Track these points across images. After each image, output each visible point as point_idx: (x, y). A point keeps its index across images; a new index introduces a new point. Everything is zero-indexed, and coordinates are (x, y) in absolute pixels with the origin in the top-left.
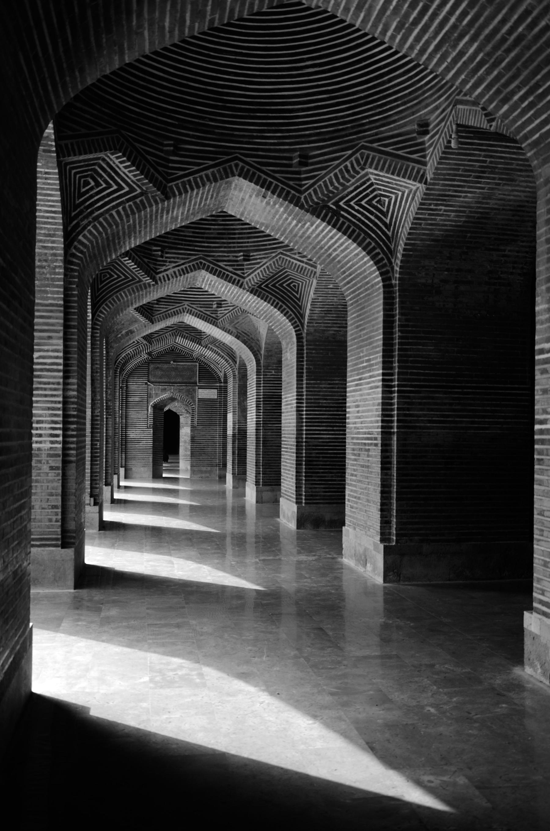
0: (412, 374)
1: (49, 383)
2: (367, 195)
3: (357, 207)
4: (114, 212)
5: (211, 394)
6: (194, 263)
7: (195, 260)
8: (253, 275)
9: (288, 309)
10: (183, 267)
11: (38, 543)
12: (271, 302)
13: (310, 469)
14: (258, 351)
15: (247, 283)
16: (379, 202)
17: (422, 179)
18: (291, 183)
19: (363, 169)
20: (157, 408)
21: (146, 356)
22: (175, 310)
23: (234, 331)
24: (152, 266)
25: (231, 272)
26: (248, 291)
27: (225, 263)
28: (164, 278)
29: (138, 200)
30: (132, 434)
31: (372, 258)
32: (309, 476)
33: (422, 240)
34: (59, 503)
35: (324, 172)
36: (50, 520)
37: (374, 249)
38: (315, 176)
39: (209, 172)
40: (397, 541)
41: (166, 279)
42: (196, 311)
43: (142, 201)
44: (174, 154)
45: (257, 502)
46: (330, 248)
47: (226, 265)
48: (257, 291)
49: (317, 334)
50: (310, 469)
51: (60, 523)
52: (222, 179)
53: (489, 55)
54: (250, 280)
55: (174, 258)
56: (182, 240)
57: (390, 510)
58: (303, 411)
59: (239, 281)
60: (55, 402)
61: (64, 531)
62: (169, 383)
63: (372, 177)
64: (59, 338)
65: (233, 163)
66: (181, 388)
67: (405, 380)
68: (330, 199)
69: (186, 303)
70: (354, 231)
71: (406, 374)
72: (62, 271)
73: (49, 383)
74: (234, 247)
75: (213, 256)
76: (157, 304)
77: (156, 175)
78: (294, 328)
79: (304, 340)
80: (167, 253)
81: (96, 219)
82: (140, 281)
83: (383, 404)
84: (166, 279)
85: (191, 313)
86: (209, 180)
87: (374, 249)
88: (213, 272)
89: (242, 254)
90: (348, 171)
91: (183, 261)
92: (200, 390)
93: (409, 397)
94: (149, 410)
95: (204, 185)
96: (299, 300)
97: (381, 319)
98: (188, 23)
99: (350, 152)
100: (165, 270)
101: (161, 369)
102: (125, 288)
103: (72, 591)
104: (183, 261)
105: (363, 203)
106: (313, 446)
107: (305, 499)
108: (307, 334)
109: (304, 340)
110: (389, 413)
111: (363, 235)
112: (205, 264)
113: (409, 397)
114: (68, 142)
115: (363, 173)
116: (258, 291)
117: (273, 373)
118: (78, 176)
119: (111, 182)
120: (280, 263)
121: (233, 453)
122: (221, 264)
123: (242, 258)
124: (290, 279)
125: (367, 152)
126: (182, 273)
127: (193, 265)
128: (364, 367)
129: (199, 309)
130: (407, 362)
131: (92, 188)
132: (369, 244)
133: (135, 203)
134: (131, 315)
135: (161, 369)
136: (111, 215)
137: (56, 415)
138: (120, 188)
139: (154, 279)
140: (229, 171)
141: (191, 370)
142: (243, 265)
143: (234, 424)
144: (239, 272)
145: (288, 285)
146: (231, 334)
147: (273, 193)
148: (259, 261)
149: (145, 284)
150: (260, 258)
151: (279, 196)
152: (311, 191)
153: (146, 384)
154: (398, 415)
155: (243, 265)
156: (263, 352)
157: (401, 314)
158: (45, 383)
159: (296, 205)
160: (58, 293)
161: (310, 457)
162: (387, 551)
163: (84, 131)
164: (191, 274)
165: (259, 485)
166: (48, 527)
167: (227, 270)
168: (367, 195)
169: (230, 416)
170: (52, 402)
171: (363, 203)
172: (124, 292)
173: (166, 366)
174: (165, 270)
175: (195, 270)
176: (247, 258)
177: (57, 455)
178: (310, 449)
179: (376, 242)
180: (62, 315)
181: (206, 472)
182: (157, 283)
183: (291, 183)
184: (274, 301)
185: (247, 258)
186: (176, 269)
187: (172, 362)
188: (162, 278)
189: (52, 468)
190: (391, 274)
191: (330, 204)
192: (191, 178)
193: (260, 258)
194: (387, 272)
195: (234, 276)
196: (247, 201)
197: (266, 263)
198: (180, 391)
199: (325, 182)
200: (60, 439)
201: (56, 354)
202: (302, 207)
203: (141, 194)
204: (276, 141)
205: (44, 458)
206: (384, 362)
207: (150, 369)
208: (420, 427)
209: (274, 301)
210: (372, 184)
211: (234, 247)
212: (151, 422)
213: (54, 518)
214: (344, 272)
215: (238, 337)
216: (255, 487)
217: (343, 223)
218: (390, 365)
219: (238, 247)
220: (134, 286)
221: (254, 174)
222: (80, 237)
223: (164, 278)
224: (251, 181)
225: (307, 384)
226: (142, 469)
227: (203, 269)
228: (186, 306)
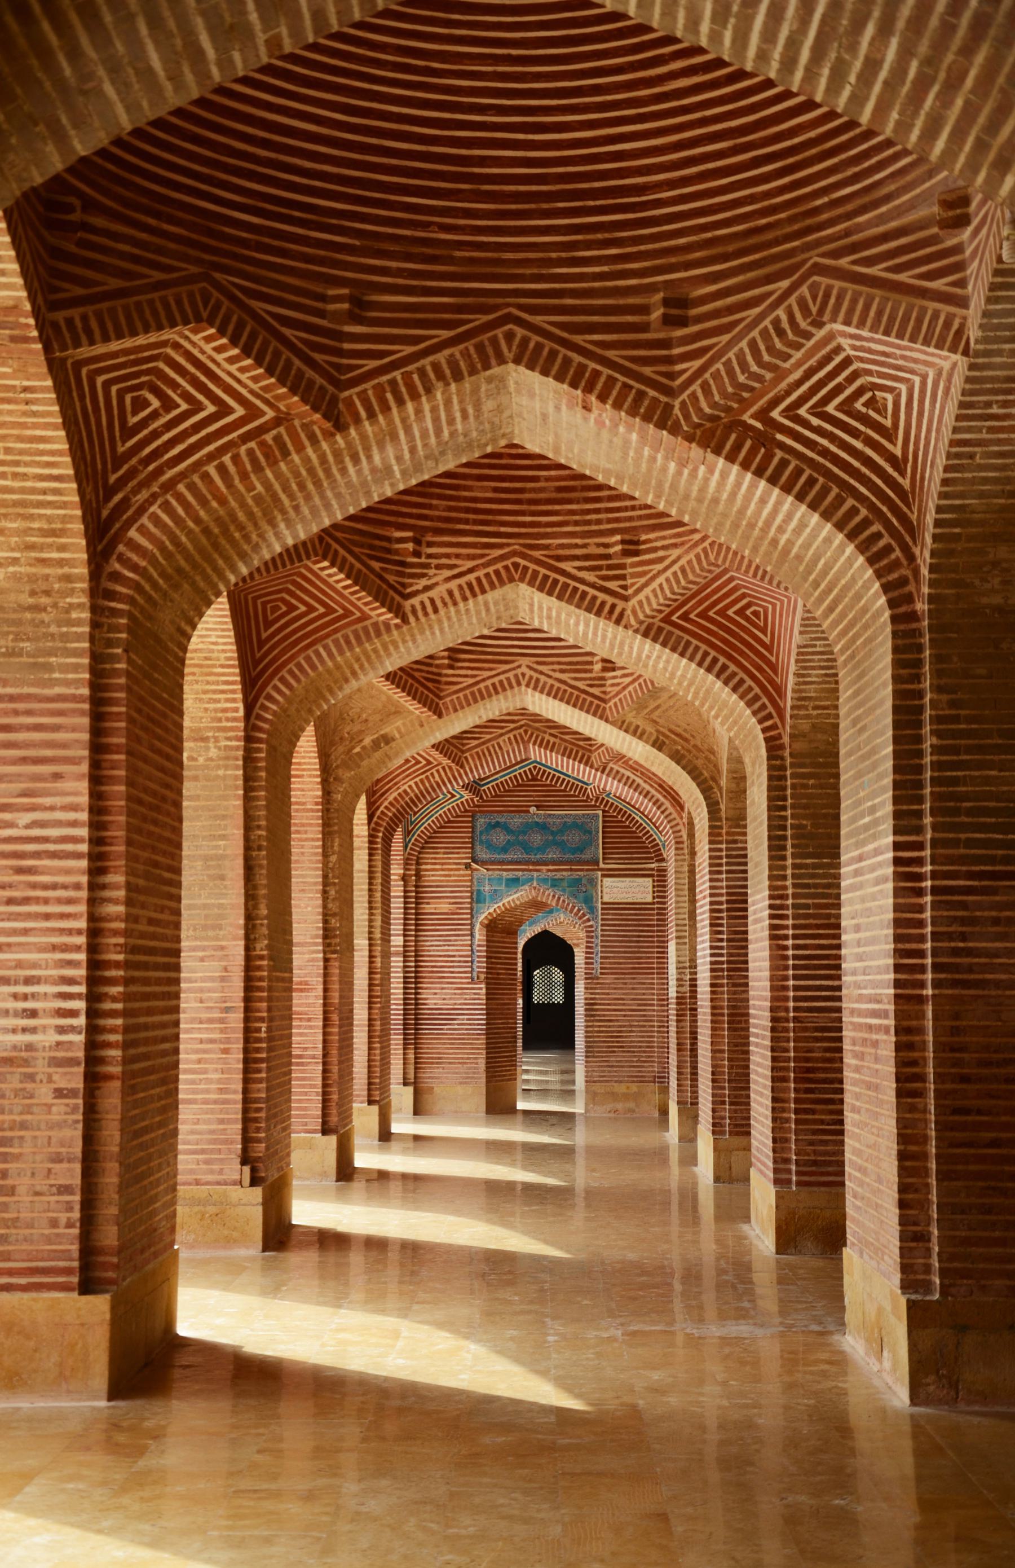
0: (969, 843)
1: (54, 887)
2: (838, 389)
3: (815, 421)
4: (211, 469)
5: (635, 890)
6: (499, 566)
7: (502, 558)
8: (648, 591)
9: (741, 675)
10: (471, 577)
11: (23, 1281)
12: (698, 657)
13: (808, 1091)
14: (714, 779)
15: (634, 612)
16: (871, 403)
17: (957, 342)
18: (647, 371)
19: (819, 324)
20: (500, 930)
21: (467, 795)
22: (496, 680)
23: (650, 729)
24: (391, 578)
25: (593, 586)
26: (636, 631)
27: (577, 564)
28: (424, 608)
29: (268, 437)
31: (862, 549)
32: (806, 1111)
33: (981, 495)
34: (77, 1181)
35: (725, 338)
36: (54, 1223)
37: (866, 523)
38: (705, 350)
39: (441, 357)
40: (944, 1290)
41: (430, 609)
42: (550, 681)
43: (277, 439)
44: (356, 319)
45: (717, 1179)
46: (768, 524)
47: (580, 569)
48: (660, 629)
49: (819, 736)
50: (808, 1091)
51: (76, 1231)
52: (473, 371)
53: (931, 62)
54: (640, 603)
55: (448, 556)
56: (467, 510)
57: (924, 1205)
58: (786, 937)
59: (613, 606)
60: (70, 932)
61: (88, 1250)
62: (527, 862)
63: (845, 342)
64: (79, 777)
65: (499, 332)
66: (559, 875)
67: (950, 860)
68: (745, 404)
69: (525, 661)
70: (811, 482)
71: (956, 843)
72: (86, 615)
73: (54, 887)
74: (599, 522)
75: (547, 547)
76: (451, 667)
77: (310, 373)
78: (760, 722)
79: (787, 753)
80: (430, 544)
81: (169, 486)
82: (365, 617)
83: (897, 923)
84: (430, 609)
85: (535, 686)
86: (440, 376)
87: (866, 523)
88: (547, 587)
89: (618, 537)
90: (781, 333)
91: (470, 564)
92: (607, 881)
93: (964, 906)
94: (477, 936)
95: (429, 390)
96: (769, 648)
97: (889, 704)
98: (211, 53)
99: (785, 284)
100: (427, 588)
101: (506, 828)
102: (327, 636)
103: (103, 1403)
104: (470, 564)
105: (830, 408)
106: (817, 1029)
107: (798, 1173)
108: (792, 736)
109: (787, 753)
110: (914, 946)
111: (835, 490)
112: (526, 568)
113: (964, 906)
114: (75, 313)
115: (820, 334)
116: (665, 630)
118: (114, 389)
119: (200, 397)
120: (712, 557)
122: (567, 566)
123: (618, 548)
124: (744, 596)
125: (824, 281)
126: (468, 593)
127: (497, 572)
128: (866, 827)
130: (956, 812)
131: (155, 415)
132: (853, 511)
133: (262, 444)
134: (384, 698)
135: (506, 828)
136: (206, 477)
137: (70, 963)
138: (225, 409)
139: (398, 611)
140: (490, 351)
141: (584, 828)
142: (623, 566)
144: (613, 585)
145: (740, 612)
146: (640, 738)
147: (602, 398)
148: (661, 553)
149: (375, 625)
150: (664, 548)
151: (617, 405)
152: (696, 387)
153: (468, 866)
154: (935, 952)
155: (623, 566)
156: (723, 782)
157: (937, 689)
158: (46, 887)
159: (661, 425)
160: (76, 668)
161: (807, 1060)
162: (917, 1316)
163: (115, 283)
164: (491, 596)
166: (49, 1240)
167: (582, 581)
168: (838, 389)
170: (62, 931)
171: (830, 408)
172: (326, 647)
174: (427, 588)
175: (502, 583)
176: (632, 548)
177: (72, 1062)
178: (807, 1039)
179: (872, 507)
180: (86, 721)
181: (626, 1097)
182: (405, 620)
183: (647, 371)
184: (706, 654)
185: (632, 548)
186: (453, 585)
187: (533, 810)
188: (419, 607)
189: (59, 1093)
190: (911, 587)
191: (747, 418)
192: (397, 374)
193: (664, 548)
194: (903, 582)
195: (602, 596)
196: (549, 417)
197: (679, 558)
198: (555, 883)
199: (728, 364)
200: (81, 1021)
201: (72, 816)
202: (675, 430)
203: (277, 422)
204: (605, 269)
205: (41, 1068)
206: (897, 815)
207: (478, 829)
208: (997, 984)
209: (706, 654)
210: (847, 362)
211: (599, 522)
212: (480, 965)
213: (63, 1217)
214: (816, 584)
215: (658, 745)
217: (784, 464)
218: (914, 822)
219: (609, 521)
220: (349, 631)
221: (553, 354)
222: (133, 533)
223: (424, 608)
224: (545, 373)
225: (795, 866)
226: (460, 1089)
227: (522, 580)
228: (524, 669)
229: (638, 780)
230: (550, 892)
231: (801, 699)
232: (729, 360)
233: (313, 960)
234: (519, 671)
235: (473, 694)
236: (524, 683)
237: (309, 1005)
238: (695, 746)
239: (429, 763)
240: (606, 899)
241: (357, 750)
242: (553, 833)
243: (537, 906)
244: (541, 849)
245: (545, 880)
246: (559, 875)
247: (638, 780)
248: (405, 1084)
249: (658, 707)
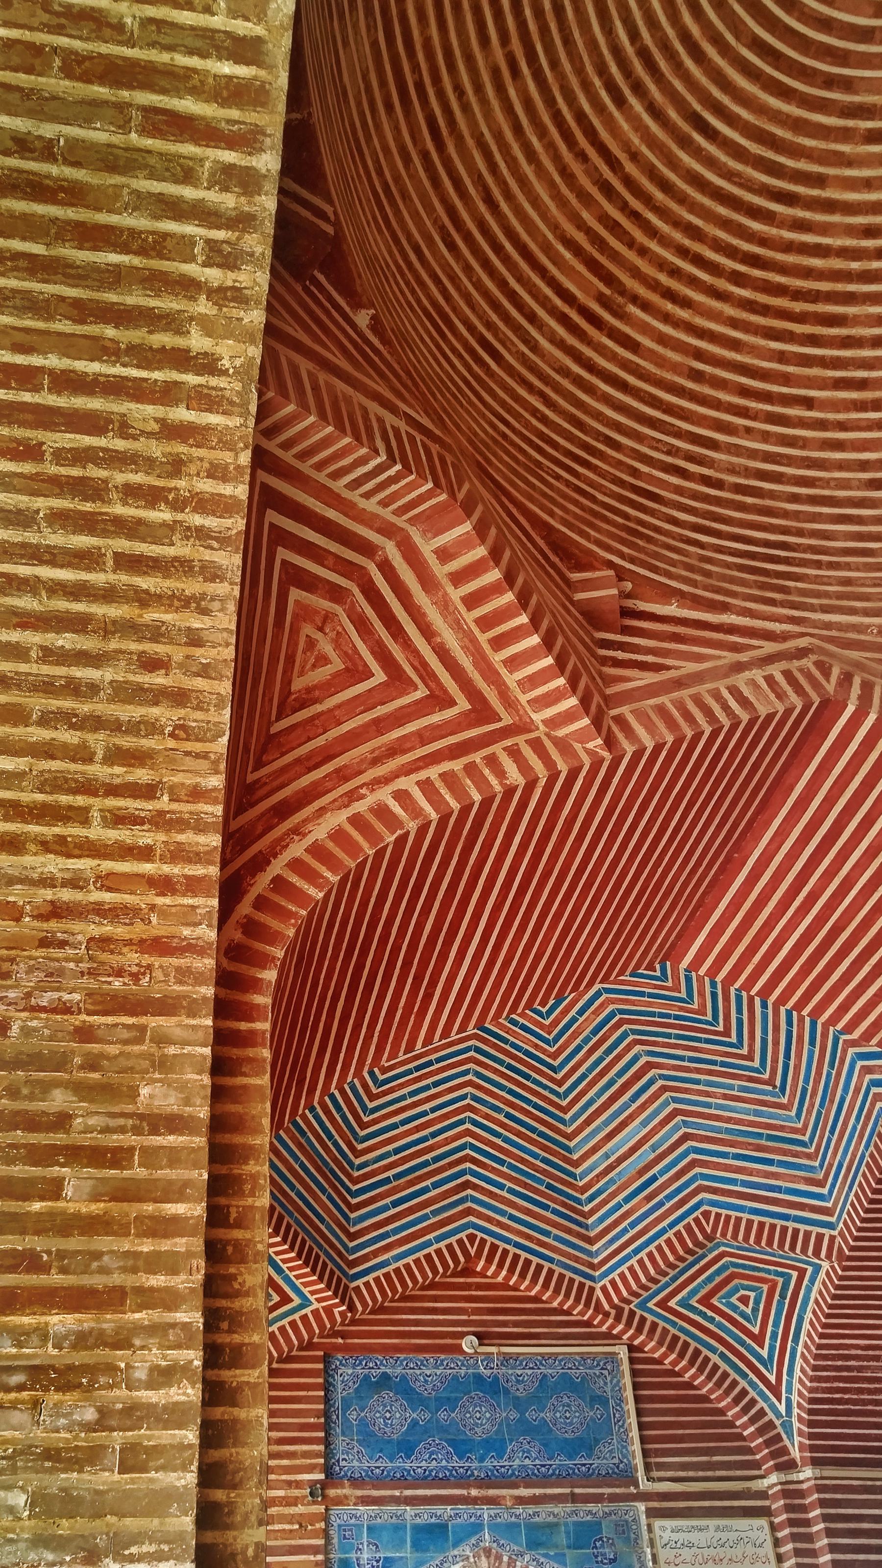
62: (463, 1481)
66: (544, 1513)
101: (404, 1389)
135: (404, 1389)
173: (429, 1372)
187: (468, 1344)
207: (340, 1393)
242: (518, 1404)
244: (494, 1446)
246: (544, 1513)
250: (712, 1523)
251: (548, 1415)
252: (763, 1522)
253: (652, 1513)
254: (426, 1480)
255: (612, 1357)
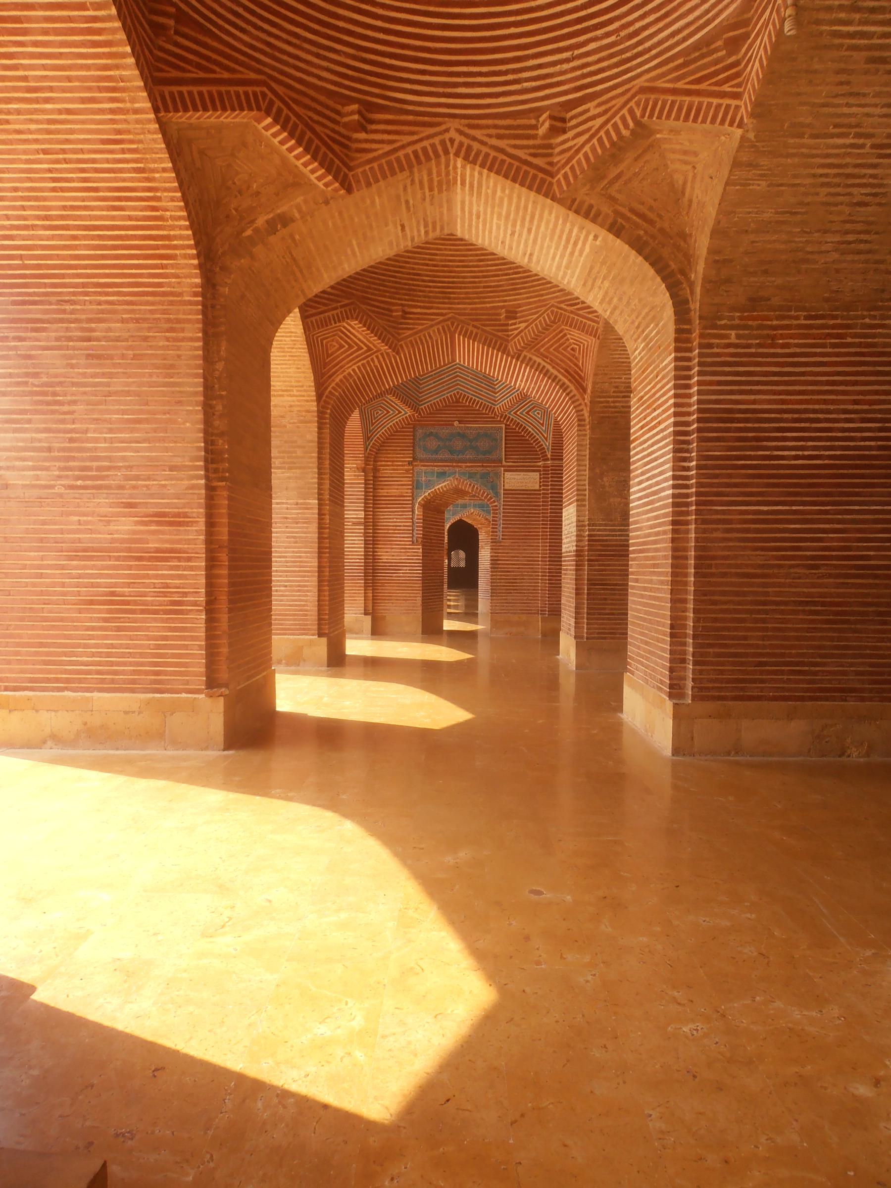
5: (529, 480)
14: (683, 272)
20: (433, 509)
22: (418, 147)
23: (606, 209)
30: (386, 555)
42: (485, 149)
45: (676, 751)
66: (474, 470)
69: (454, 124)
92: (508, 475)
101: (437, 436)
117: (733, 340)
121: (578, 592)
129: (494, 142)
135: (437, 436)
143: (580, 526)
146: (594, 220)
153: (410, 463)
165: (682, 696)
169: (569, 514)
173: (444, 432)
187: (456, 423)
198: (471, 476)
212: (419, 533)
216: (669, 705)
228: (453, 134)
229: (548, 367)
230: (468, 482)
231: (718, 259)
232: (580, 159)
233: (193, 487)
234: (447, 136)
235: (389, 163)
236: (452, 151)
237: (188, 542)
238: (662, 230)
239: (369, 349)
240: (506, 487)
241: (249, 232)
243: (459, 493)
245: (464, 474)
246: (474, 470)
247: (548, 367)
248: (366, 614)
249: (619, 176)
250: (522, 473)
251: (478, 444)
252: (538, 474)
253: (505, 471)
254: (442, 461)
255: (501, 428)
